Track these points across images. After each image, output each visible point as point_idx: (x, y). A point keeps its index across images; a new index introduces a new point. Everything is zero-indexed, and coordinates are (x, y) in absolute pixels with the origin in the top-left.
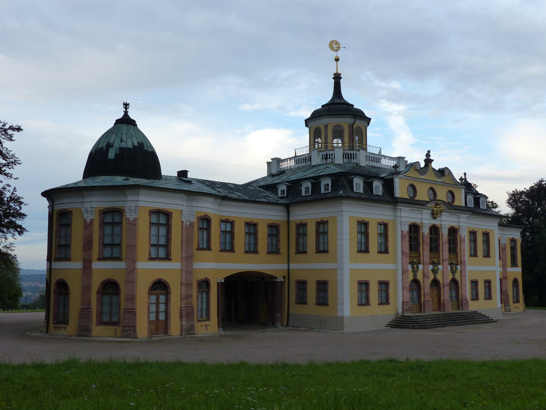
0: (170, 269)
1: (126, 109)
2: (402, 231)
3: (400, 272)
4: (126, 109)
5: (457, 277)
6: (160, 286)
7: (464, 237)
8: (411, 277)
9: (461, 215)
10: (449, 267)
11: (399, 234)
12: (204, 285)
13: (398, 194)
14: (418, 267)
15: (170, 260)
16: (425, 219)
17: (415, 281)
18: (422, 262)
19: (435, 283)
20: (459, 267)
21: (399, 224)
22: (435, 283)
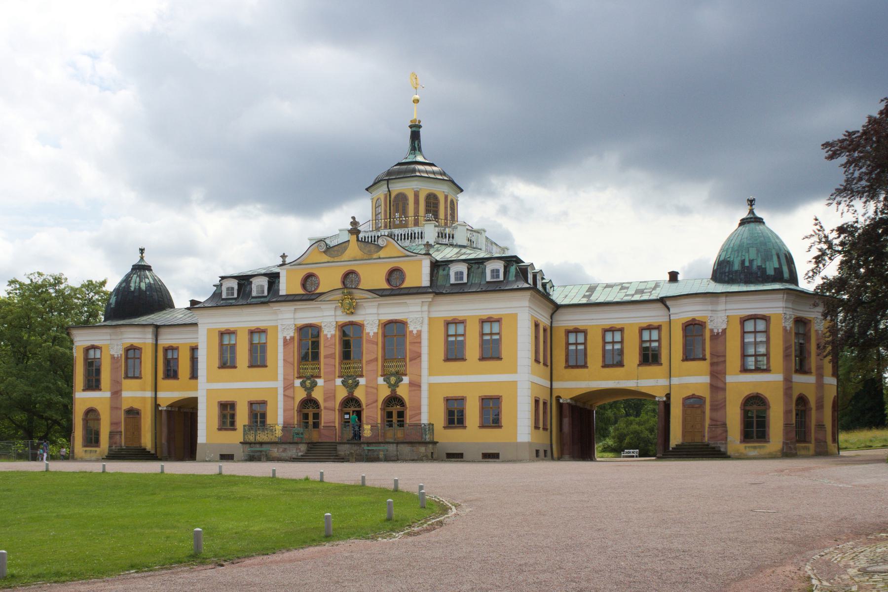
0: (99, 398)
1: (142, 253)
2: (285, 339)
3: (281, 391)
4: (142, 253)
5: (403, 391)
6: (91, 414)
7: (419, 332)
8: (301, 395)
9: (408, 301)
10: (381, 380)
11: (281, 343)
12: (133, 413)
13: (283, 290)
14: (314, 384)
15: (100, 390)
16: (327, 318)
17: (309, 403)
18: (322, 375)
19: (351, 402)
20: (406, 380)
21: (279, 330)
22: (351, 402)
